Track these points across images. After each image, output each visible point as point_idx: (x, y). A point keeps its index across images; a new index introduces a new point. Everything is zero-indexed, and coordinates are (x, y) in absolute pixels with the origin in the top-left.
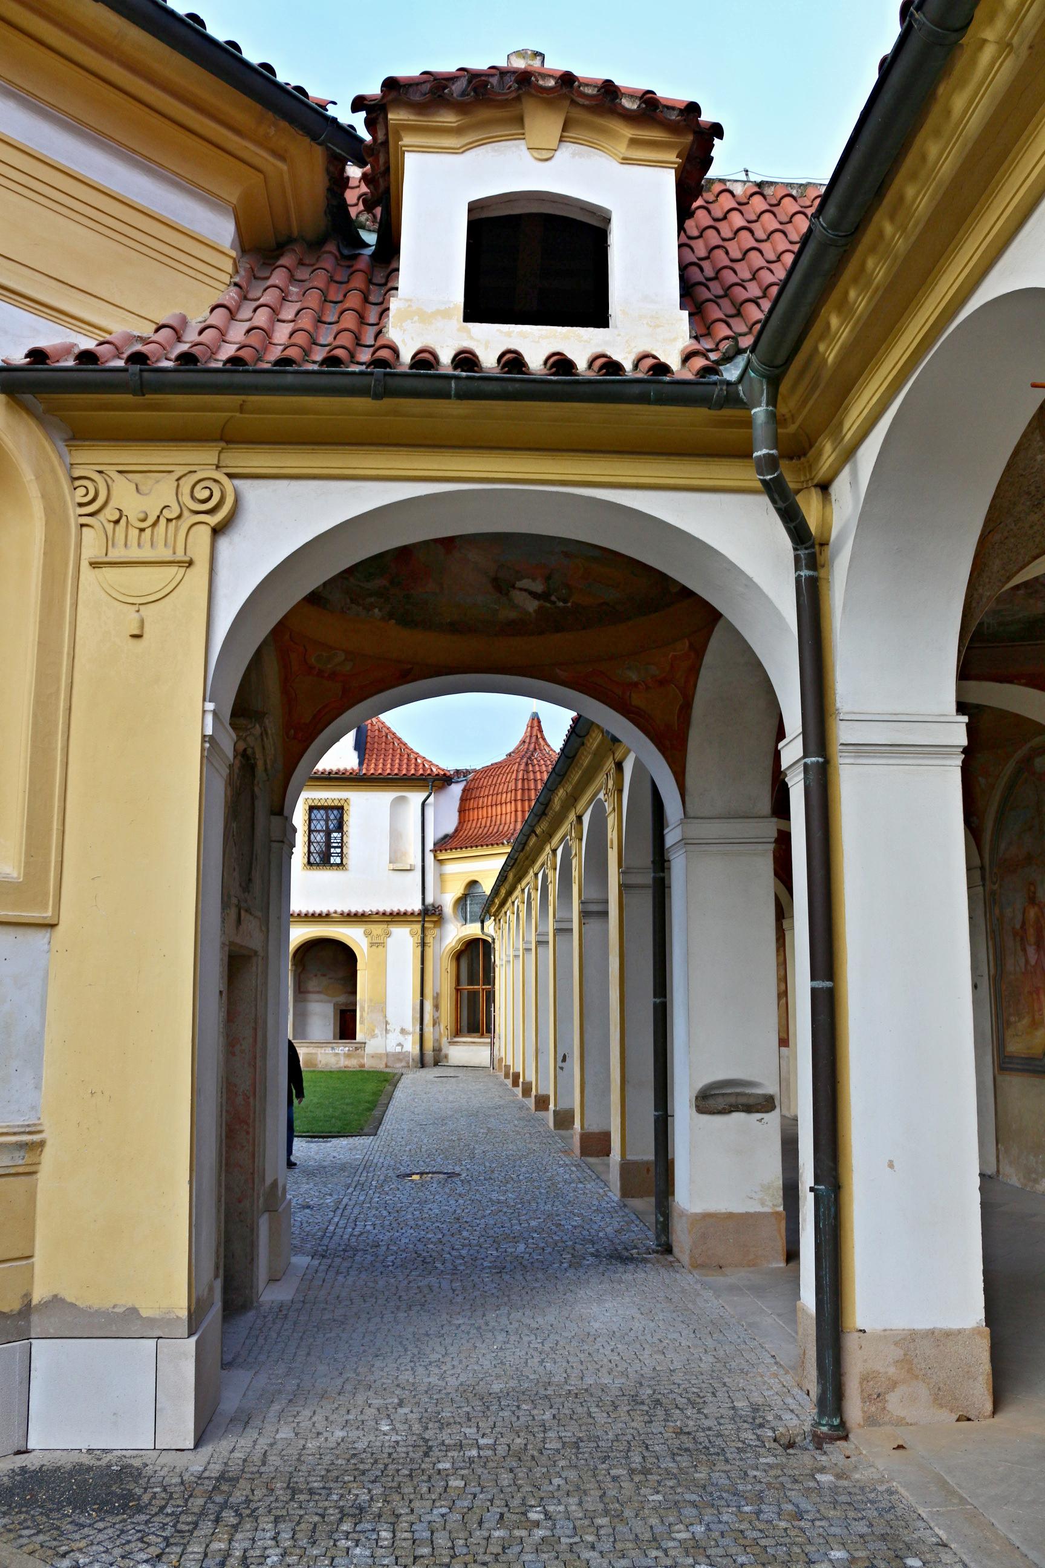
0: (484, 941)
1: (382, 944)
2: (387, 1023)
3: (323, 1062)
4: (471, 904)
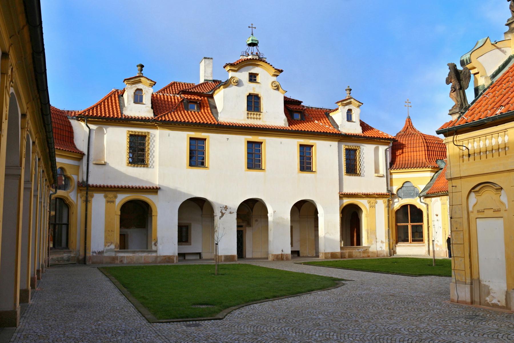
1: (374, 207)
2: (376, 239)
3: (355, 255)
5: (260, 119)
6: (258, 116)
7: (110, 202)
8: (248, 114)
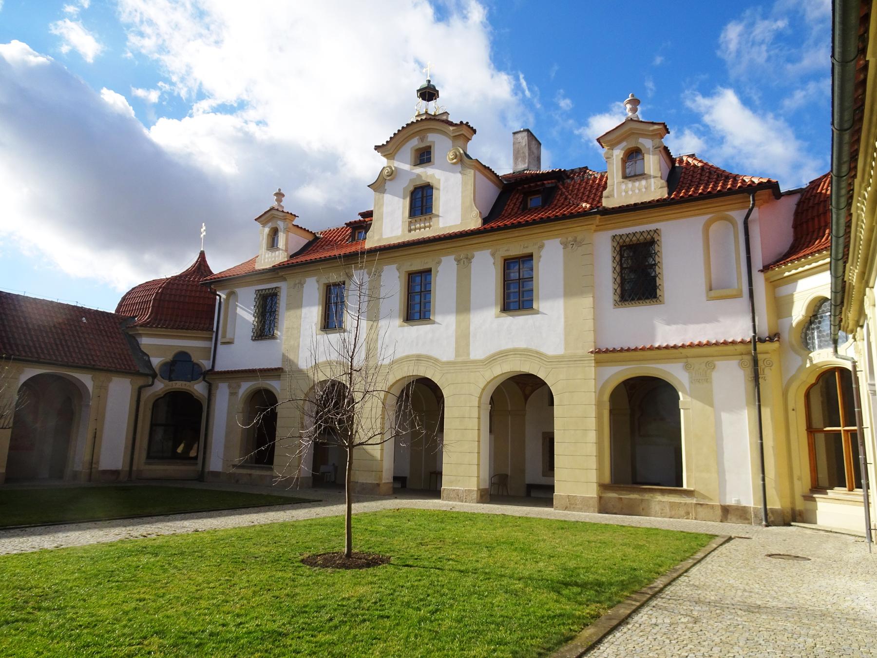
0: (843, 371)
4: (819, 337)
5: (430, 227)
6: (427, 224)
7: (233, 394)
8: (410, 223)
